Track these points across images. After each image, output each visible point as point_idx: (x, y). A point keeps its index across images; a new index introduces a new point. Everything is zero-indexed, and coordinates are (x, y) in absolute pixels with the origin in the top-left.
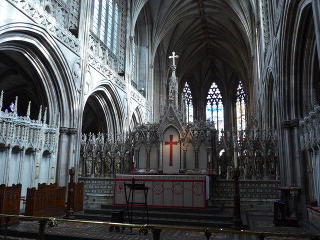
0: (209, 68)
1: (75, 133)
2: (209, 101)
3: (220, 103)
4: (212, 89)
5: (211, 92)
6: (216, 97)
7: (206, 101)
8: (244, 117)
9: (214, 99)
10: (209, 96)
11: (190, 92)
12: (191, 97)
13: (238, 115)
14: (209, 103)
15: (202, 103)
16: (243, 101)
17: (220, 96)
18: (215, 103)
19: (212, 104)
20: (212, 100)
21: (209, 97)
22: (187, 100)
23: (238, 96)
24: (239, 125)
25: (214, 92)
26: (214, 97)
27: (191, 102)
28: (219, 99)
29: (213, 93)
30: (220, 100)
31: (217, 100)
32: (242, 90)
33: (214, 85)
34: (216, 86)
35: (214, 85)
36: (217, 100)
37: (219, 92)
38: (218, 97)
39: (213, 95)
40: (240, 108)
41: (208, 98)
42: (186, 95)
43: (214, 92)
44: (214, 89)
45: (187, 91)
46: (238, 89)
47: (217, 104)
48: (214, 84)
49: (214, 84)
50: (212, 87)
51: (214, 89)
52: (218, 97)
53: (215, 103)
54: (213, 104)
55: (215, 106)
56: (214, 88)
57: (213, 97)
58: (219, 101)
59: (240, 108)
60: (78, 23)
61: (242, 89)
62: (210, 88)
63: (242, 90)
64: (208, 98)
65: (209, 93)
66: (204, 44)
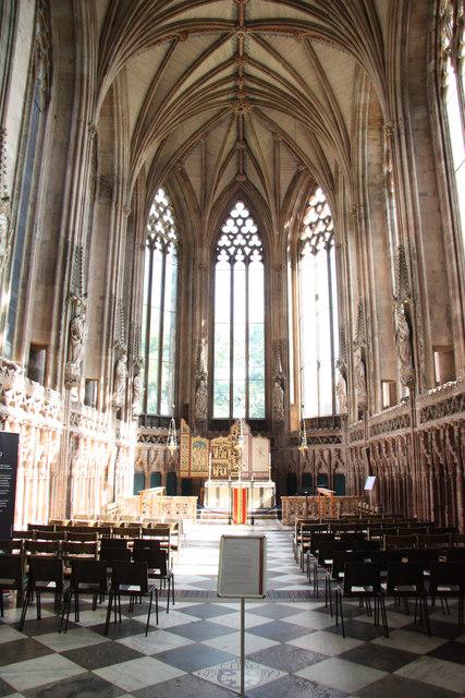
0: (232, 152)
3: (256, 257)
4: (235, 219)
5: (229, 227)
6: (243, 242)
7: (215, 253)
9: (238, 247)
10: (224, 238)
11: (172, 222)
12: (172, 235)
14: (223, 257)
15: (205, 253)
17: (256, 241)
18: (240, 257)
19: (232, 261)
20: (232, 250)
21: (224, 241)
22: (162, 241)
23: (309, 240)
25: (240, 228)
26: (240, 240)
27: (172, 250)
28: (254, 247)
29: (235, 230)
30: (256, 252)
31: (247, 250)
33: (240, 210)
34: (246, 213)
35: (240, 210)
36: (247, 250)
37: (254, 229)
38: (251, 244)
39: (235, 236)
41: (221, 243)
42: (159, 227)
43: (240, 228)
45: (161, 215)
47: (247, 261)
50: (234, 214)
52: (251, 244)
53: (240, 257)
54: (235, 261)
55: (240, 265)
57: (236, 242)
58: (251, 254)
59: (313, 276)
62: (229, 216)
65: (225, 229)
66: (227, 49)
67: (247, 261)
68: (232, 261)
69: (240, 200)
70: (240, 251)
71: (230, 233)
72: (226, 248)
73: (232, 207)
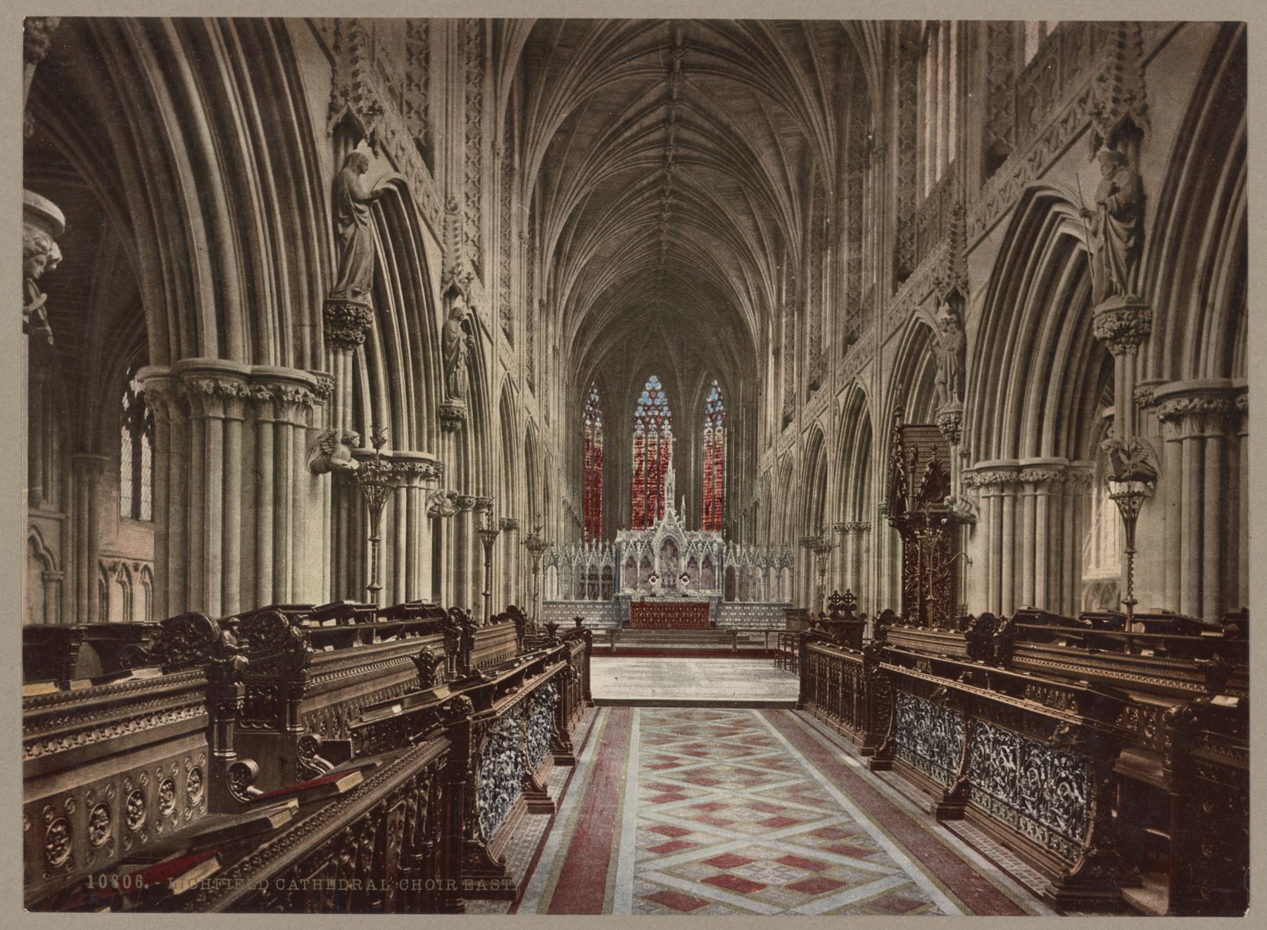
2: (639, 421)
3: (667, 427)
4: (650, 392)
5: (644, 398)
7: (635, 419)
10: (640, 408)
14: (640, 426)
17: (666, 412)
21: (640, 412)
28: (665, 417)
29: (650, 402)
30: (666, 422)
32: (720, 403)
33: (654, 383)
35: (654, 383)
41: (637, 414)
46: (709, 400)
48: (653, 378)
49: (653, 378)
50: (648, 386)
56: (653, 390)
58: (663, 424)
60: (532, 377)
61: (719, 399)
63: (720, 403)
64: (637, 414)
69: (653, 373)
70: (653, 421)
71: (645, 405)
72: (643, 419)
73: (646, 380)
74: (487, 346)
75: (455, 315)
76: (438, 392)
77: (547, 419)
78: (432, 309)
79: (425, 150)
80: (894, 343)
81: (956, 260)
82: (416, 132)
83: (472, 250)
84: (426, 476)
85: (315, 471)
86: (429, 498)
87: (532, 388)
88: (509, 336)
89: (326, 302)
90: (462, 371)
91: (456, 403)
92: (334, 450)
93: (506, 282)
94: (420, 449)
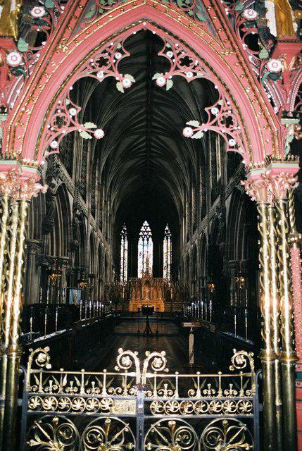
1: (102, 281)
3: (150, 239)
5: (143, 229)
7: (139, 236)
8: (169, 253)
13: (165, 251)
14: (141, 239)
16: (169, 240)
17: (150, 234)
18: (145, 239)
19: (143, 240)
21: (141, 234)
24: (165, 260)
26: (146, 233)
28: (150, 236)
33: (146, 223)
35: (146, 223)
40: (167, 245)
44: (146, 227)
47: (148, 240)
48: (146, 222)
49: (146, 222)
50: (144, 225)
51: (146, 227)
53: (145, 239)
59: (167, 245)
67: (148, 240)
68: (143, 240)
74: (86, 221)
75: (76, 215)
76: (71, 238)
77: (106, 239)
78: (70, 215)
79: (70, 172)
80: (211, 222)
81: (222, 202)
82: (67, 165)
83: (82, 192)
84: (66, 263)
85: (37, 267)
86: (66, 270)
87: (101, 229)
88: (94, 216)
89: (43, 222)
90: (79, 232)
91: (76, 242)
92: (42, 261)
93: (93, 197)
94: (65, 255)
